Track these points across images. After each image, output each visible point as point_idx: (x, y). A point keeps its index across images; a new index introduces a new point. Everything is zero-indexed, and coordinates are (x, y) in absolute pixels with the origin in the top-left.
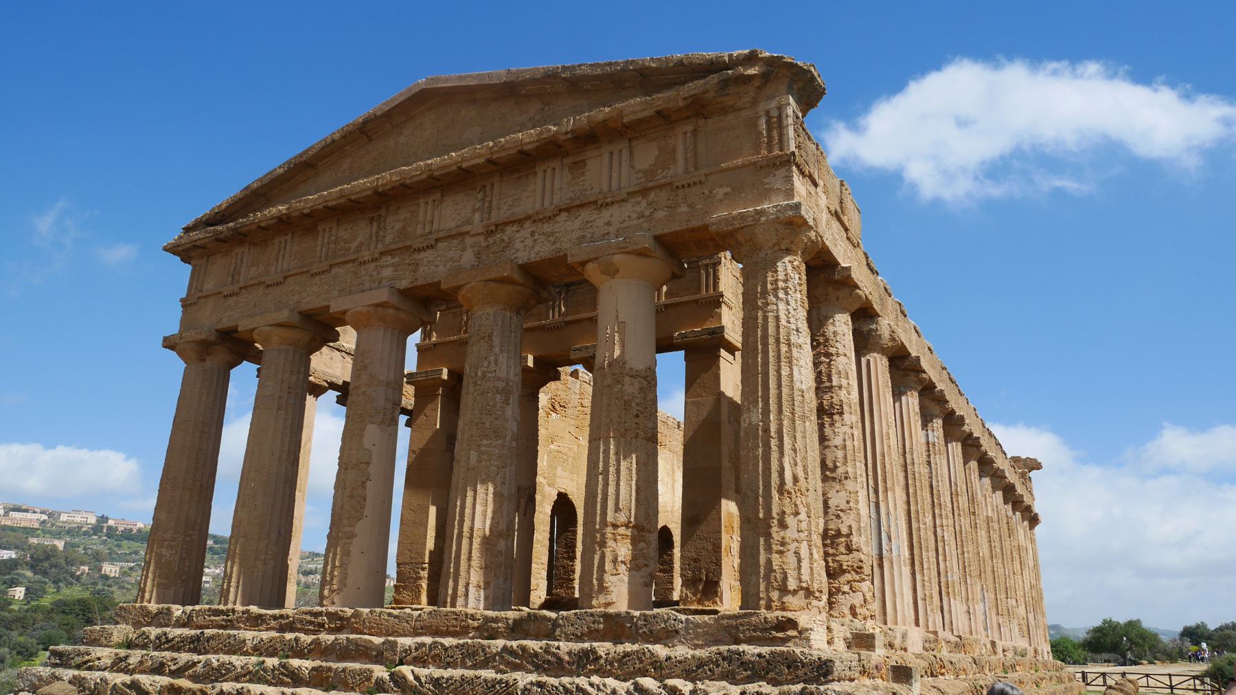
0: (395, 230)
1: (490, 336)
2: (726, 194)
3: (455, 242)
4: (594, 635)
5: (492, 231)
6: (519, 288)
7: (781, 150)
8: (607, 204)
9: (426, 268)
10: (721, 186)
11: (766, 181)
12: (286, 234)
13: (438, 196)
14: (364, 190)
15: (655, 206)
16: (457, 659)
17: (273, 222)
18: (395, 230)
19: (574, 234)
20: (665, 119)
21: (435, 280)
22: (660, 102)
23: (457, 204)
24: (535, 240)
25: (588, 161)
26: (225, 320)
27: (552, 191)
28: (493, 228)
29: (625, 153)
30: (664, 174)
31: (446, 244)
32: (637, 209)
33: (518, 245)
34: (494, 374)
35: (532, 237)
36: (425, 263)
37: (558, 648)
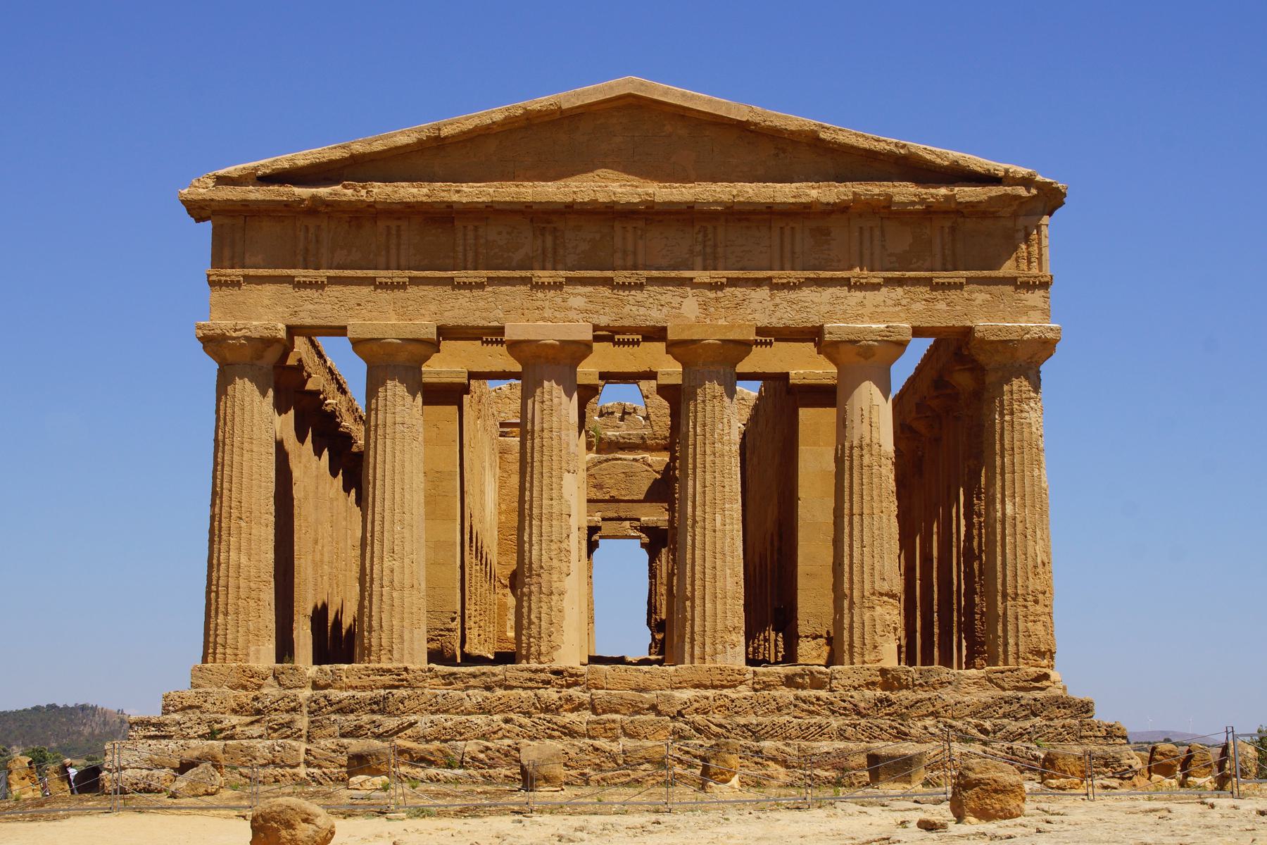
4: (871, 685)
7: (1041, 270)
9: (634, 308)
12: (399, 219)
13: (641, 224)
17: (399, 206)
20: (930, 212)
23: (667, 238)
26: (302, 315)
27: (793, 253)
29: (877, 233)
30: (919, 264)
33: (755, 305)
35: (772, 299)
37: (852, 697)
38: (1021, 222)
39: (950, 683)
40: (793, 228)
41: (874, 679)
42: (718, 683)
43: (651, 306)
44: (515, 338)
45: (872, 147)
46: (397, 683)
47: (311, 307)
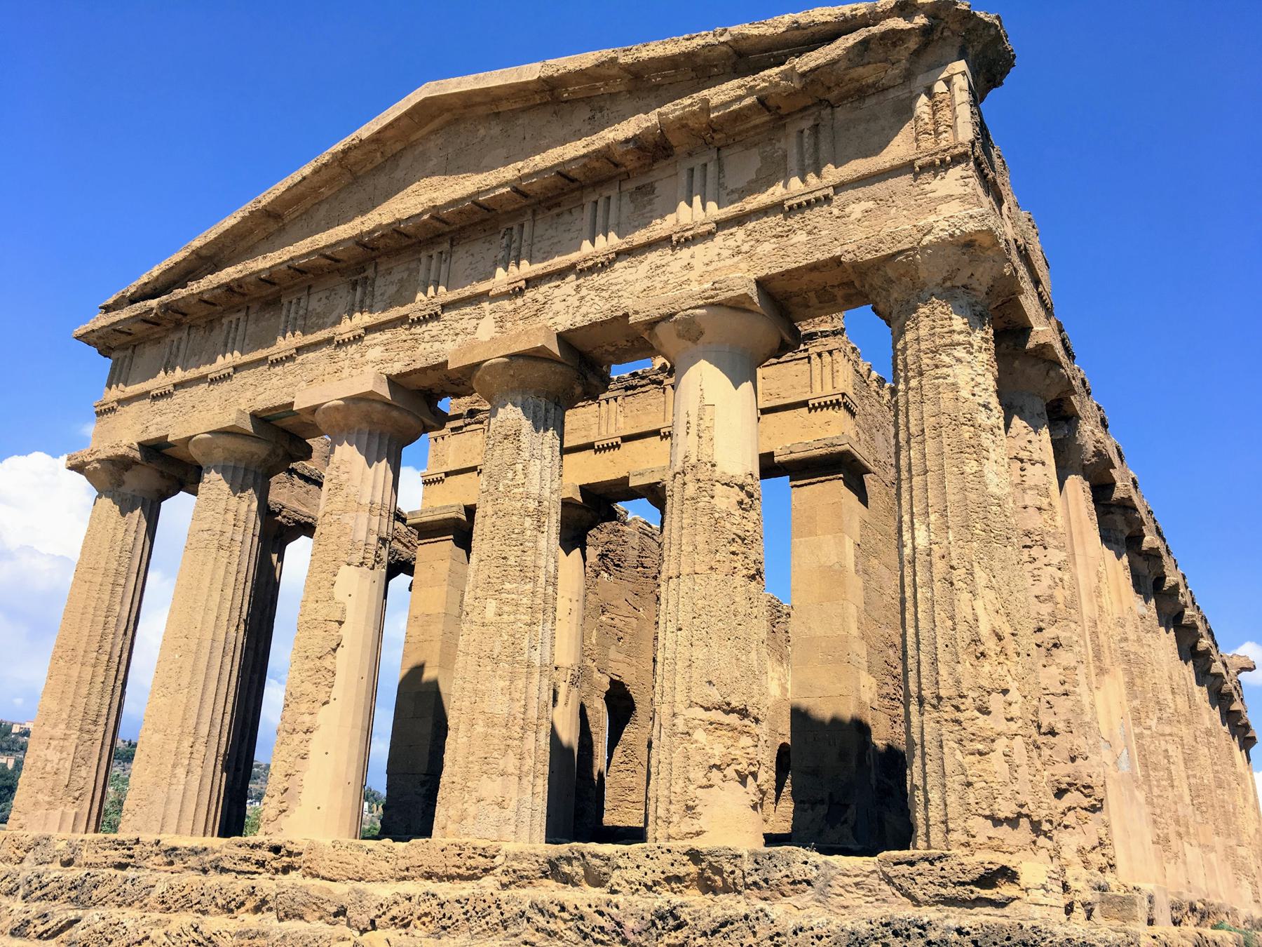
0: (387, 295)
1: (517, 434)
5: (520, 289)
6: (559, 368)
8: (687, 240)
9: (428, 346)
12: (239, 311)
15: (758, 237)
16: (457, 921)
19: (637, 285)
21: (441, 360)
23: (472, 255)
24: (583, 298)
25: (656, 185)
28: (522, 284)
31: (454, 313)
32: (731, 243)
33: (558, 306)
34: (521, 489)
36: (427, 337)
38: (920, 81)
39: (809, 883)
42: (453, 871)
43: (446, 338)
45: (683, 49)
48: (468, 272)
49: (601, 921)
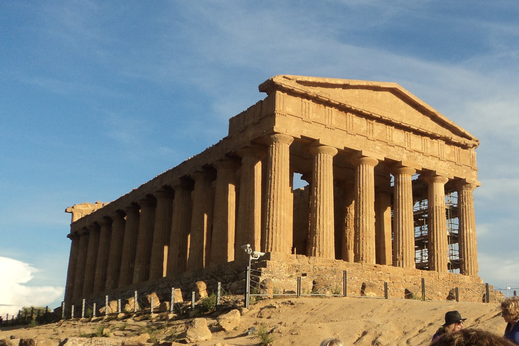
2: (465, 172)
3: (401, 149)
10: (464, 169)
11: (472, 173)
14: (379, 115)
18: (378, 132)
22: (460, 140)
31: (397, 148)
32: (447, 165)
33: (419, 160)
36: (391, 151)
40: (427, 140)
41: (447, 276)
44: (365, 155)
46: (333, 265)
47: (307, 130)
48: (398, 139)
49: (446, 283)
